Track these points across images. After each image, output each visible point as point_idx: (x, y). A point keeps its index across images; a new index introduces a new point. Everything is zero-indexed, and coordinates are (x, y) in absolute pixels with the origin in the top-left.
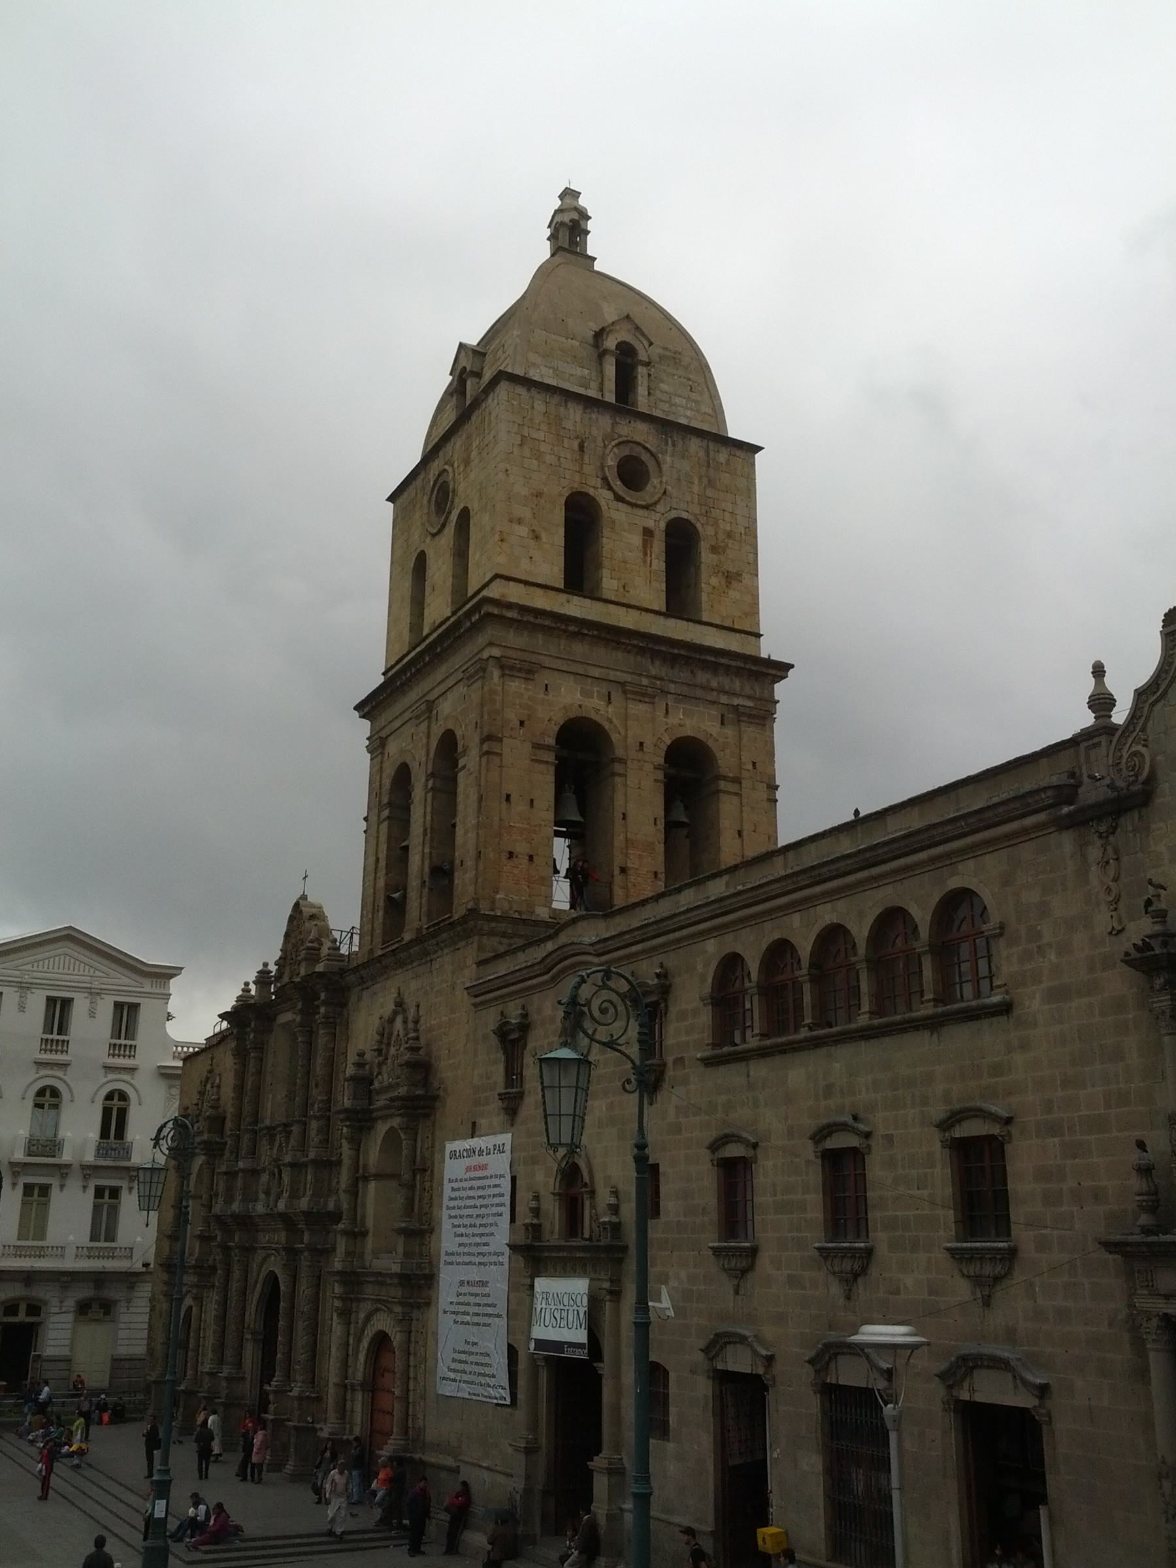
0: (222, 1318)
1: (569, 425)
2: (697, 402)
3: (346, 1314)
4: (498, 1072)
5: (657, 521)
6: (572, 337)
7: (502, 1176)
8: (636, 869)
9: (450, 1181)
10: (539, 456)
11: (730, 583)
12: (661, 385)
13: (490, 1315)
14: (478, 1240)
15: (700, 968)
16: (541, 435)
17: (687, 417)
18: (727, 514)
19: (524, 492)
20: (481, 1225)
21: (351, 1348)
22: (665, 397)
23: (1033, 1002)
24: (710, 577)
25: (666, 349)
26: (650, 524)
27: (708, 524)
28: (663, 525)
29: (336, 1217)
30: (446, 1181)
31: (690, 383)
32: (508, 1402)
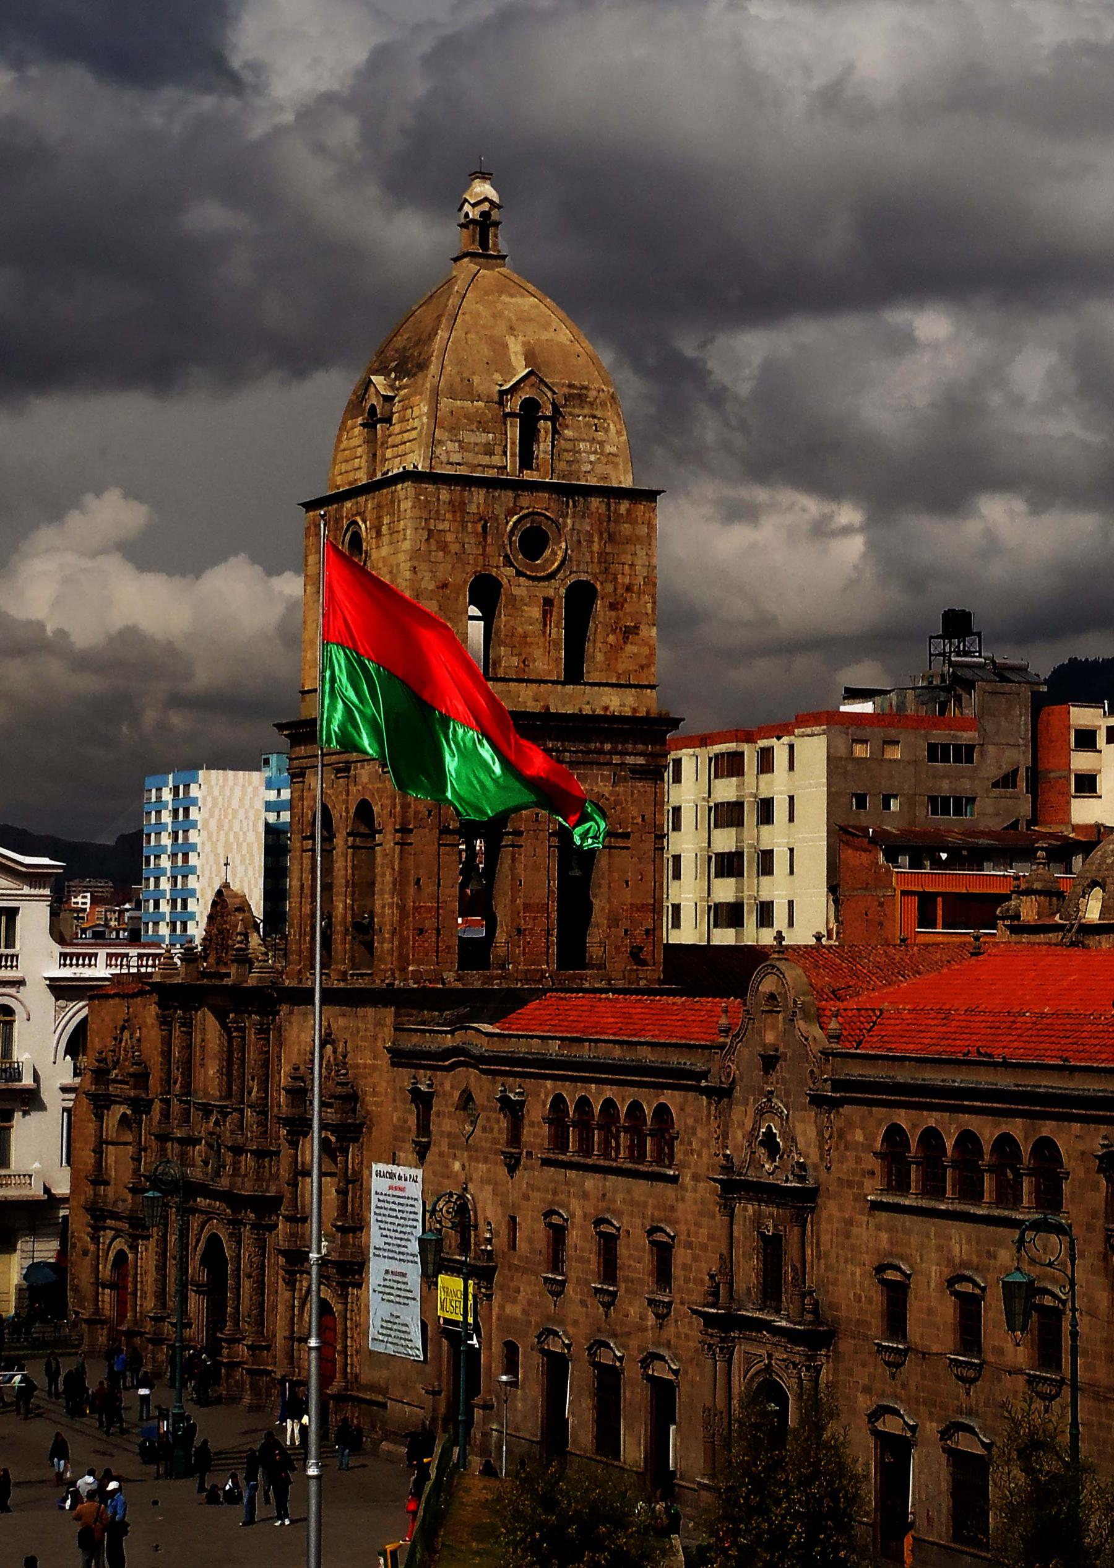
0: (161, 1268)
1: (473, 508)
2: (601, 443)
3: (291, 1284)
4: (412, 1121)
5: (557, 590)
6: (477, 398)
7: (416, 1199)
8: (531, 929)
9: (377, 1193)
10: (444, 547)
11: (628, 638)
12: (566, 432)
13: (408, 1298)
14: (398, 1242)
15: (543, 1096)
16: (446, 526)
17: (591, 462)
18: (626, 567)
19: (431, 586)
20: (401, 1232)
21: (296, 1309)
22: (569, 445)
23: (687, 1180)
24: (608, 635)
25: (571, 386)
26: (551, 592)
27: (606, 581)
28: (563, 591)
29: (277, 1200)
30: (373, 1192)
31: (596, 421)
32: (422, 1358)
